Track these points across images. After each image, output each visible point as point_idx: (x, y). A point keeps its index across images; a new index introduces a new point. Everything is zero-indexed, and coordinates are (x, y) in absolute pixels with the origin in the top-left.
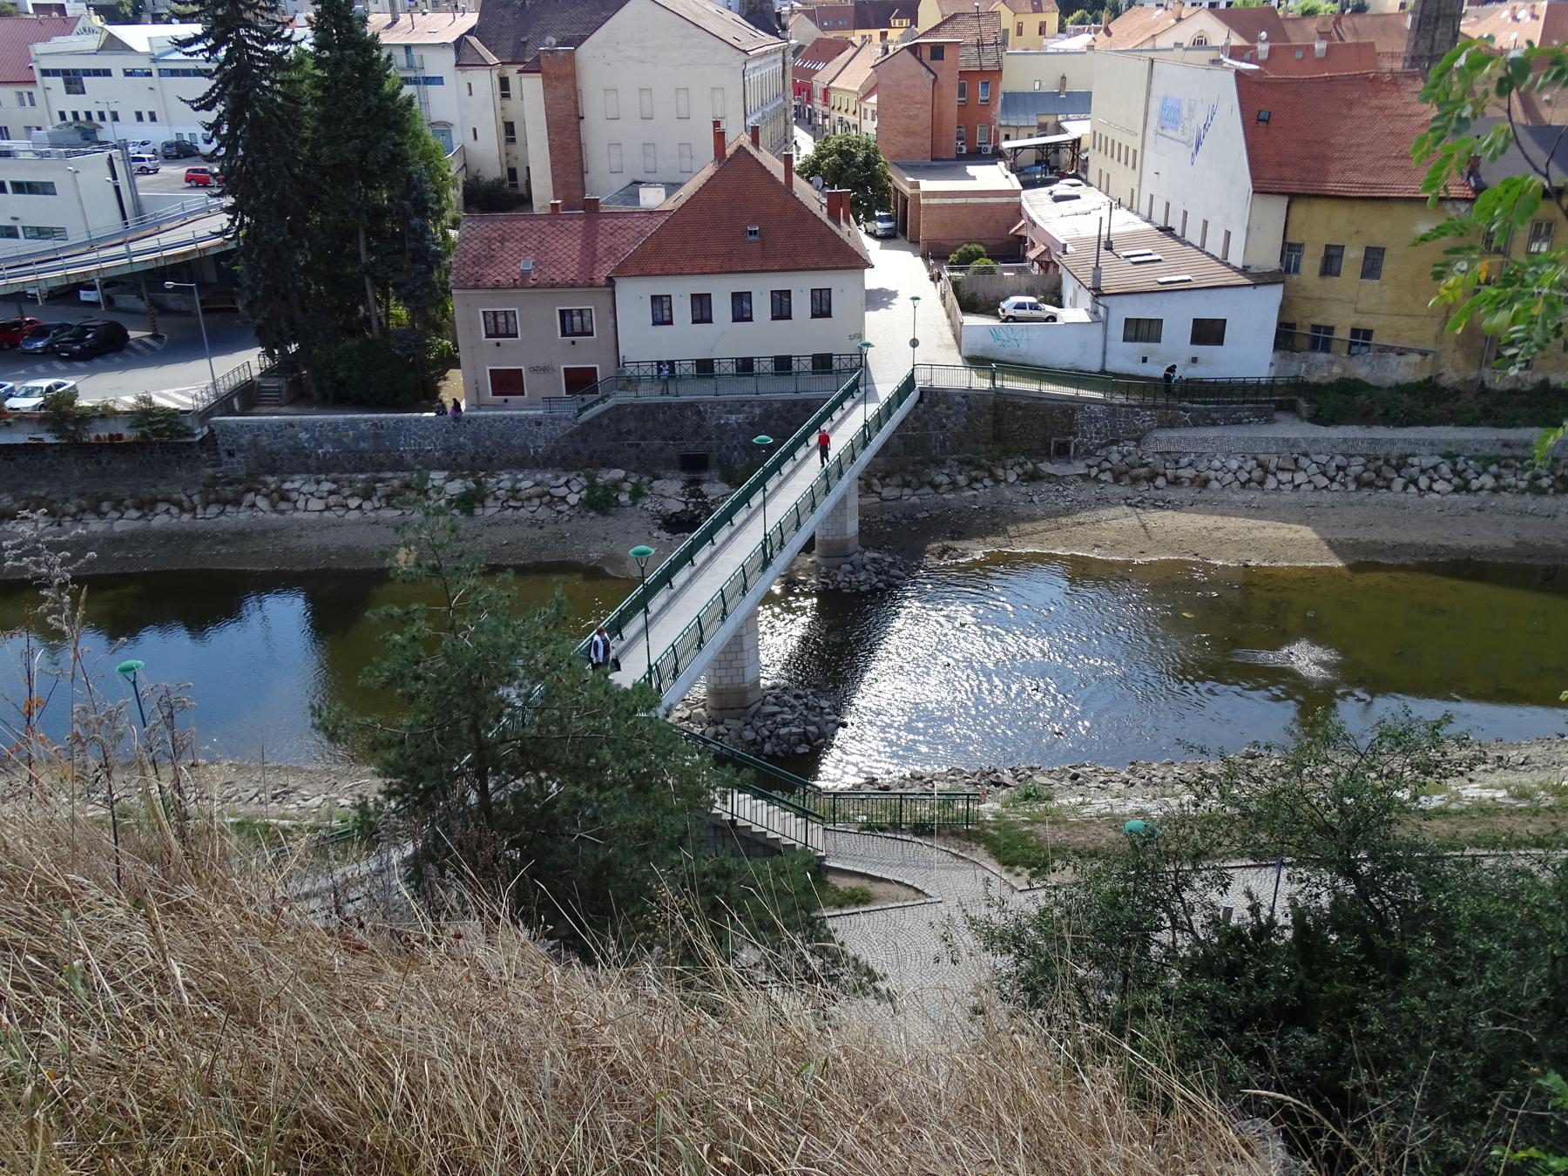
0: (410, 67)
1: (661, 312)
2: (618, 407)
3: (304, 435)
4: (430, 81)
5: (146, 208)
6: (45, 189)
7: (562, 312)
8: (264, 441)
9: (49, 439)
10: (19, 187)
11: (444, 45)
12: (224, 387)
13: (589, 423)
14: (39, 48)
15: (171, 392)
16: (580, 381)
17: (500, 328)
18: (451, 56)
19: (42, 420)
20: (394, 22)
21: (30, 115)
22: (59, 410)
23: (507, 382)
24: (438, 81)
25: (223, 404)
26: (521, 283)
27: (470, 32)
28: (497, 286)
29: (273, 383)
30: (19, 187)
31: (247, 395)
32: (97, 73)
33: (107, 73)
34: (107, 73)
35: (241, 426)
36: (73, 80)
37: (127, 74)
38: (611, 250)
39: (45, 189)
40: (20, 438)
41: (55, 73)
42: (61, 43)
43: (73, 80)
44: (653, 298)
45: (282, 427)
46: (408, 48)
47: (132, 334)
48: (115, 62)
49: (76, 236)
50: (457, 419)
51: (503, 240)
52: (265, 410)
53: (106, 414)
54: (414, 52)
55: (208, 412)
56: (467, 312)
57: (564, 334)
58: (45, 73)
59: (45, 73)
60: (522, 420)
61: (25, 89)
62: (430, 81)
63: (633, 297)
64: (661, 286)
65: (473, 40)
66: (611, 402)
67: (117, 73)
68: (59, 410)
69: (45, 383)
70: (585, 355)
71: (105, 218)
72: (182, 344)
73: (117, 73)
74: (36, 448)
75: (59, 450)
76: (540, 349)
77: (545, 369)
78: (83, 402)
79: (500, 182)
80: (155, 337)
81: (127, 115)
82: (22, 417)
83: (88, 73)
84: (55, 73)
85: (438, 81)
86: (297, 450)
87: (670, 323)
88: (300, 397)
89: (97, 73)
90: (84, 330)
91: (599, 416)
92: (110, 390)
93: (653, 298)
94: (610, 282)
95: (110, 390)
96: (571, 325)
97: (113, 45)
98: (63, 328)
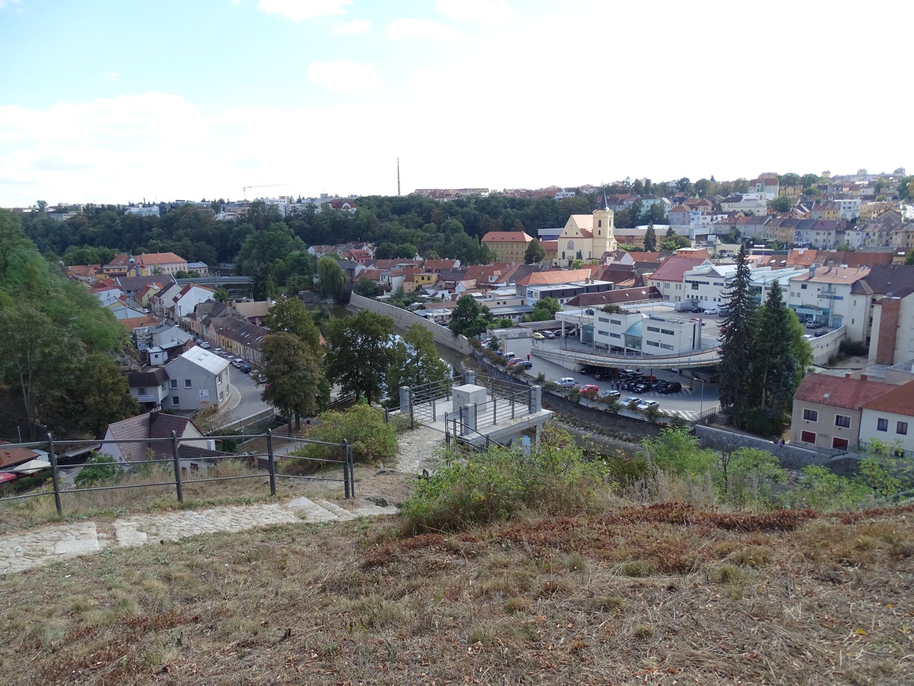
0: (829, 291)
1: (882, 426)
2: (849, 459)
3: (725, 438)
4: (838, 298)
5: (702, 342)
6: (672, 333)
7: (838, 417)
8: (711, 436)
9: (646, 420)
10: (663, 331)
11: (847, 285)
12: (704, 415)
13: (835, 462)
14: (688, 272)
15: (687, 412)
16: (840, 444)
17: (810, 416)
18: (849, 289)
19: (646, 414)
20: (829, 271)
21: (679, 293)
22: (652, 412)
23: (809, 437)
24: (841, 298)
25: (702, 421)
26: (823, 402)
27: (863, 279)
28: (812, 401)
29: (722, 416)
30: (663, 331)
31: (711, 419)
32: (704, 283)
33: (708, 283)
34: (708, 283)
35: (705, 430)
36: (695, 285)
37: (715, 284)
38: (866, 397)
39: (672, 333)
40: (638, 417)
41: (690, 282)
42: (696, 269)
43: (695, 285)
44: (880, 420)
45: (718, 433)
46: (830, 284)
47: (683, 386)
48: (712, 280)
49: (676, 351)
50: (781, 446)
51: (820, 384)
52: (715, 425)
53: (665, 416)
54: (833, 287)
55: (696, 422)
56: (799, 407)
57: (837, 424)
58: (687, 281)
59: (687, 281)
60: (807, 453)
61: (679, 284)
62: (838, 298)
63: (870, 418)
64: (884, 415)
65: (863, 282)
66: (846, 456)
67: (711, 283)
68: (652, 412)
69: (651, 402)
70: (843, 434)
71: (687, 345)
72: (697, 394)
73: (711, 283)
74: (642, 421)
75: (648, 423)
76: (825, 428)
77: (825, 436)
78: (660, 410)
79: (860, 343)
80: (691, 389)
81: (711, 299)
82: (641, 411)
83: (701, 283)
84: (690, 282)
85: (841, 298)
86: (721, 442)
87: (886, 430)
88: (729, 423)
89: (704, 283)
90: (668, 384)
91: (840, 460)
92: (669, 407)
93: (880, 420)
94: (861, 409)
95: (669, 407)
96: (842, 422)
97: (713, 273)
98: (663, 381)
